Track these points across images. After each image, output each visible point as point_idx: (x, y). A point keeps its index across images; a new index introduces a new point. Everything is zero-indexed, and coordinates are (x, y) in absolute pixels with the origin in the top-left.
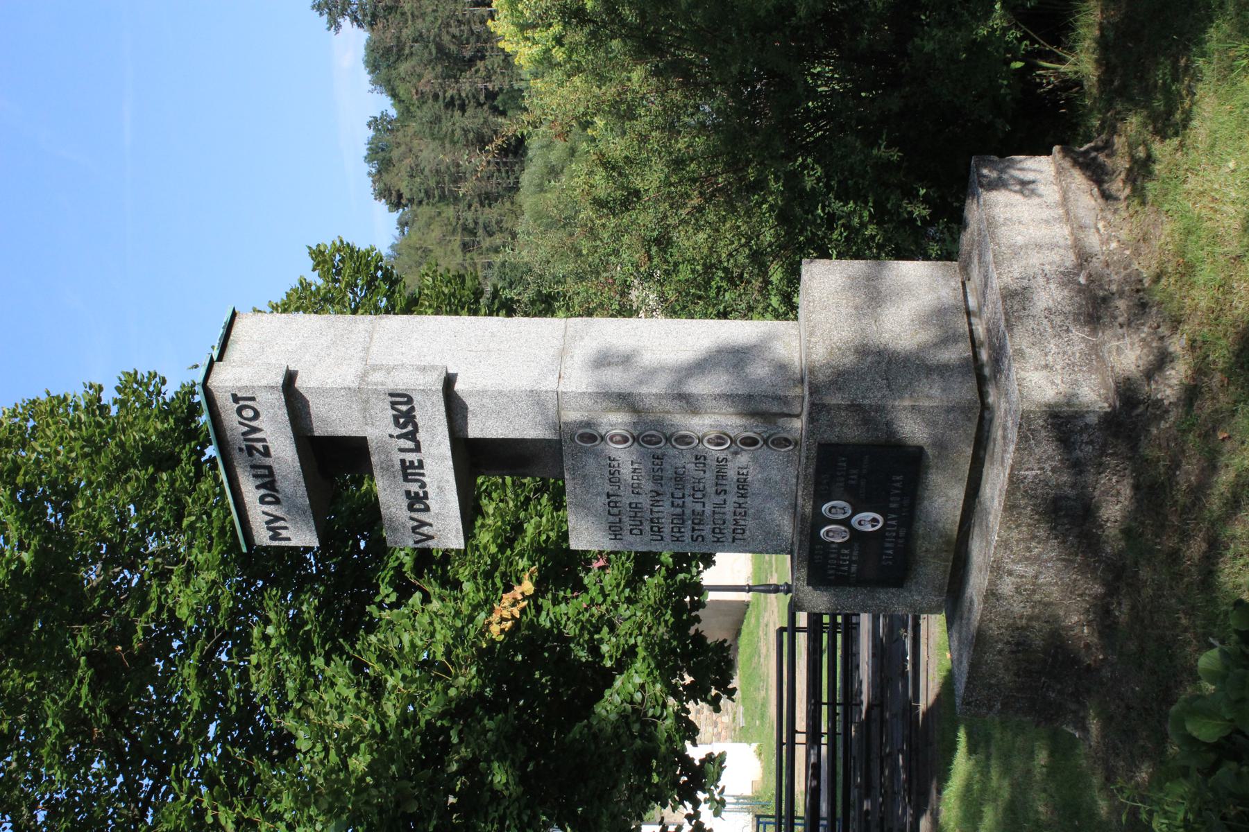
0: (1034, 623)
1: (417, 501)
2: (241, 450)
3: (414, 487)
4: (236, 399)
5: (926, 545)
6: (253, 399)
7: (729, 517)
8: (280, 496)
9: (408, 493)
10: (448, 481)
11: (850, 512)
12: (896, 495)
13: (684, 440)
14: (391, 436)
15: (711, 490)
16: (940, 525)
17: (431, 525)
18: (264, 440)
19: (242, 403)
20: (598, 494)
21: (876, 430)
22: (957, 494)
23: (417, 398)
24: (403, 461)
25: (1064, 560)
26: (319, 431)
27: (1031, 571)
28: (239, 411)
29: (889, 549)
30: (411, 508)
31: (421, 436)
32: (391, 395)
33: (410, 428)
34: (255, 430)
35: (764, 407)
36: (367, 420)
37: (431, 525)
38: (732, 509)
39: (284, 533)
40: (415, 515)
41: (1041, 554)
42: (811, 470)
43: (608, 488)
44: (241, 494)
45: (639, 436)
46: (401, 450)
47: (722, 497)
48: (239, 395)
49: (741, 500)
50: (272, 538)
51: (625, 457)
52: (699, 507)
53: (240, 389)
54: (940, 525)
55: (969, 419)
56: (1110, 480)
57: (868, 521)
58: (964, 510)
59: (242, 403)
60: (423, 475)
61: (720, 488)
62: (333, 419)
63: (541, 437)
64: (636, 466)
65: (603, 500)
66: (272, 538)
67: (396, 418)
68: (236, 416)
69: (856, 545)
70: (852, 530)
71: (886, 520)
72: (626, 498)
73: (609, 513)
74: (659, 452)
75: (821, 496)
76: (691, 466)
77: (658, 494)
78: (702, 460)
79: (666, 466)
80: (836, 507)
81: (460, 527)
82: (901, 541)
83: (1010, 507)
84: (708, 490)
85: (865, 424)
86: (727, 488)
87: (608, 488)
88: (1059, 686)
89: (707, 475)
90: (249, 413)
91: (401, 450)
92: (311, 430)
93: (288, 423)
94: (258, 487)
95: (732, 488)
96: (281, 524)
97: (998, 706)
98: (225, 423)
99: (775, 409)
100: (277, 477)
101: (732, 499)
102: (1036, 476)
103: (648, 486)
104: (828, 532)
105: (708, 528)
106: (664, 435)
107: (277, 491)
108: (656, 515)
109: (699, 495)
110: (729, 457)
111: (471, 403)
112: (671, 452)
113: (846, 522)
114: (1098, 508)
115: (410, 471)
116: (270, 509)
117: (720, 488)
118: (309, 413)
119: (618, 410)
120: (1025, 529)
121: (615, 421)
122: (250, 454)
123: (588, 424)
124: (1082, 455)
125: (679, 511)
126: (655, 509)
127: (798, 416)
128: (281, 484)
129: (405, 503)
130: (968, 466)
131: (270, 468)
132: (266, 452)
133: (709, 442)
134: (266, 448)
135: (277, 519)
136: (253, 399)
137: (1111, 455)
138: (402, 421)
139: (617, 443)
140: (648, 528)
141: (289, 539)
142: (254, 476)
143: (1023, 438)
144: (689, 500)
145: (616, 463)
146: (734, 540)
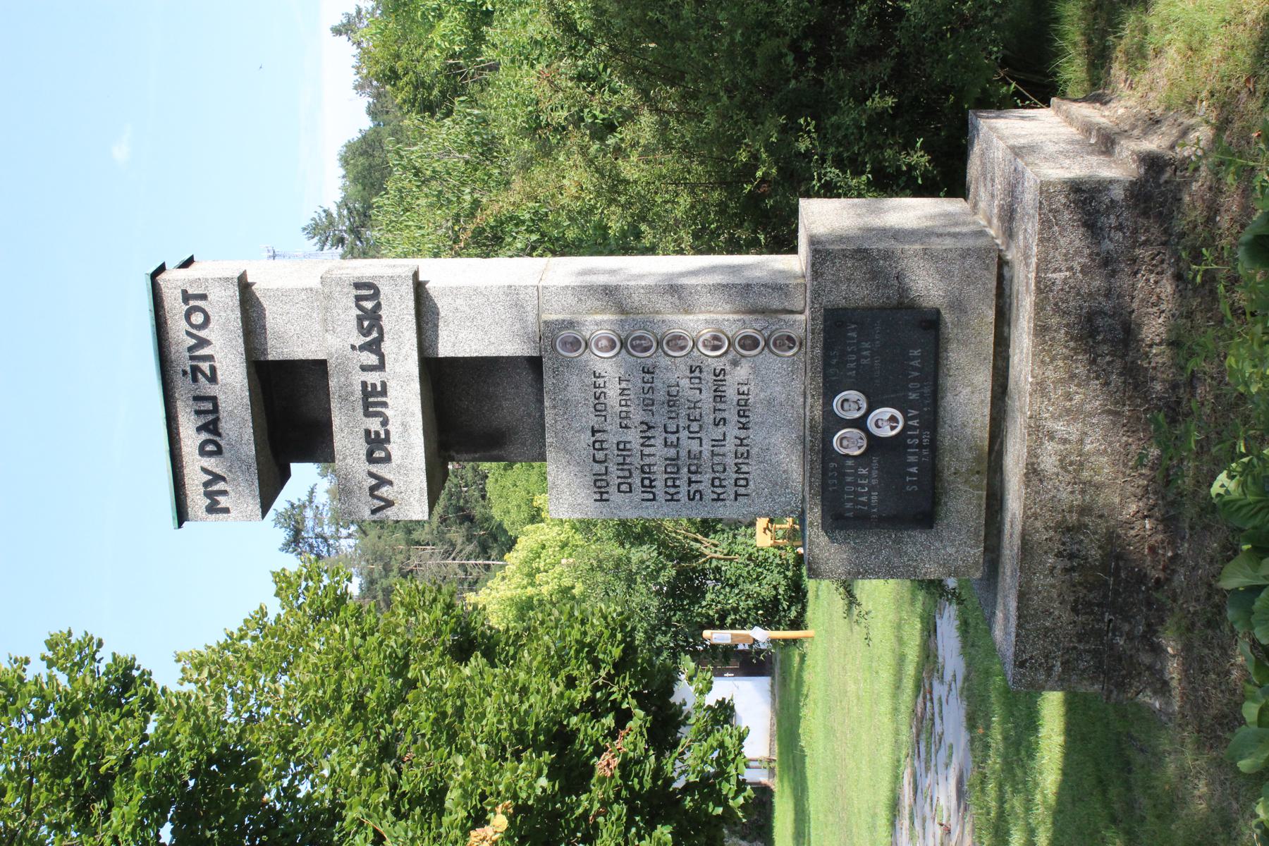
0: (1086, 519)
2: (185, 373)
3: (374, 425)
4: (186, 297)
5: (954, 465)
6: (203, 297)
7: (730, 461)
8: (222, 443)
9: (368, 432)
10: (413, 414)
11: (864, 406)
12: (914, 380)
13: (676, 342)
14: (353, 347)
15: (709, 419)
16: (968, 431)
17: (391, 483)
18: (210, 358)
19: (192, 303)
20: (582, 430)
21: (886, 286)
22: (983, 379)
23: (384, 290)
24: (364, 384)
25: (1109, 412)
26: (273, 355)
27: (1074, 431)
28: (188, 316)
29: (911, 465)
30: (371, 459)
31: (386, 346)
32: (358, 286)
33: (375, 335)
34: (203, 343)
35: (763, 302)
36: (327, 325)
37: (391, 483)
38: (733, 448)
39: (223, 501)
40: (375, 469)
41: (1083, 402)
42: (818, 351)
43: (593, 421)
44: (179, 441)
45: (627, 338)
46: (364, 368)
47: (721, 429)
48: (190, 292)
49: (743, 434)
51: (607, 367)
55: (987, 269)
56: (1148, 280)
57: (886, 422)
58: (993, 419)
59: (192, 303)
60: (385, 404)
61: (719, 415)
62: (292, 339)
63: (519, 354)
64: (624, 385)
65: (587, 438)
67: (360, 319)
68: (184, 325)
69: (875, 460)
71: (906, 419)
73: (595, 460)
74: (649, 362)
76: (685, 383)
77: (650, 428)
78: (697, 374)
79: (658, 384)
80: (850, 402)
81: (425, 485)
82: (925, 452)
83: (1041, 330)
84: (705, 418)
85: (873, 279)
86: (725, 415)
87: (593, 421)
88: (1126, 627)
89: (703, 396)
90: (198, 318)
91: (364, 368)
92: (265, 352)
93: (240, 332)
94: (199, 429)
95: (732, 416)
96: (220, 486)
97: (1058, 668)
99: (776, 304)
100: (223, 414)
101: (732, 431)
102: (1065, 281)
103: (637, 415)
104: (842, 439)
105: (707, 477)
106: (655, 335)
107: (219, 435)
108: (647, 461)
109: (695, 426)
110: (728, 368)
111: (443, 304)
112: (664, 361)
113: (860, 423)
114: (1139, 326)
115: (372, 399)
116: (210, 463)
118: (264, 327)
119: (603, 311)
120: (1060, 363)
121: (598, 324)
122: (195, 380)
123: (571, 324)
124: (1112, 247)
126: (647, 451)
127: (801, 313)
128: (224, 426)
129: (362, 448)
130: (992, 338)
131: (214, 399)
132: (213, 379)
133: (705, 346)
134: (213, 369)
135: (218, 478)
136: (203, 297)
137: (1145, 243)
138: (366, 324)
139: (601, 350)
140: (638, 481)
142: (198, 413)
143: (1045, 224)
144: (684, 434)
145: (600, 381)
146: (737, 495)
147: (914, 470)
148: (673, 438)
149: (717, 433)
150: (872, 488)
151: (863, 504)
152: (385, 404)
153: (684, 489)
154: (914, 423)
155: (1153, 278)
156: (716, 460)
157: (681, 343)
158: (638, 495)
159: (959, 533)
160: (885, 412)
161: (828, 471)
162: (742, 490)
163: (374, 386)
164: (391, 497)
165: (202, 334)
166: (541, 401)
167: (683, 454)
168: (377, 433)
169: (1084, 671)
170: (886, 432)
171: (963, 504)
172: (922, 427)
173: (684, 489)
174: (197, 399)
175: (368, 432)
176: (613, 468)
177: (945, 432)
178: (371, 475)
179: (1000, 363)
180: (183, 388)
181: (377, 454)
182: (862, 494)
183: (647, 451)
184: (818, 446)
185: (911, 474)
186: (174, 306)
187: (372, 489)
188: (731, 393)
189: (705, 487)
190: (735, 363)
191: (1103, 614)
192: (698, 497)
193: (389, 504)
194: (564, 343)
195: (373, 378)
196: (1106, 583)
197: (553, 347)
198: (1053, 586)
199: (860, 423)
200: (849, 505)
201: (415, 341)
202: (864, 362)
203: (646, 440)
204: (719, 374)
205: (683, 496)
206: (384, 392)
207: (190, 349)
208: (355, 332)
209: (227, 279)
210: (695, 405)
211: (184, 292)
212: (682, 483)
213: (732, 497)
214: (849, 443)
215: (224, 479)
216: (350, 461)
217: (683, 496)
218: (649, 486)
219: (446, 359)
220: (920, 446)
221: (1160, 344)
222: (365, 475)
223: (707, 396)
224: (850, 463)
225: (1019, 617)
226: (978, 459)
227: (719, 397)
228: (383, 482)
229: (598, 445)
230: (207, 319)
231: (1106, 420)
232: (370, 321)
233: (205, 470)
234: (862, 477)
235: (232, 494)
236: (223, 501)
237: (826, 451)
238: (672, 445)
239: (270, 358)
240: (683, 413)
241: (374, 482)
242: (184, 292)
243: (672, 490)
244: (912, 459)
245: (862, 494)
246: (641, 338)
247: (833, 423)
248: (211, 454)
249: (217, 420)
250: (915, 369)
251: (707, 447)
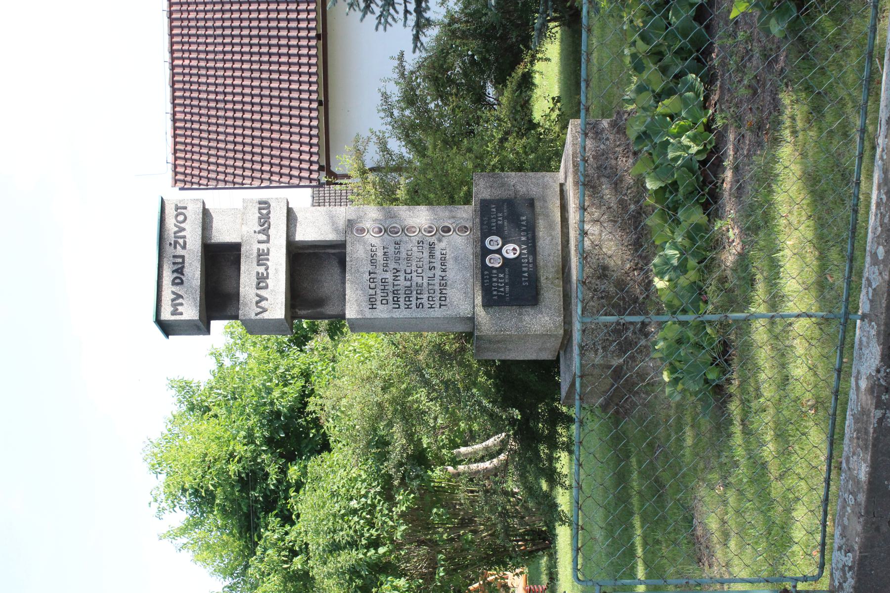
1: (261, 281)
2: (170, 244)
3: (261, 269)
6: (185, 208)
7: (437, 287)
8: (184, 279)
9: (258, 273)
13: (410, 229)
14: (255, 232)
15: (426, 267)
18: (184, 237)
23: (273, 204)
25: (612, 221)
29: (525, 272)
31: (271, 232)
32: (260, 203)
33: (266, 225)
39: (180, 309)
40: (260, 292)
46: (259, 242)
47: (433, 272)
49: (443, 274)
50: (173, 314)
52: (419, 280)
53: (180, 201)
57: (511, 251)
60: (268, 260)
61: (432, 265)
62: (223, 234)
65: (366, 276)
66: (173, 314)
67: (260, 218)
70: (504, 258)
71: (521, 250)
72: (380, 275)
74: (398, 239)
75: (484, 236)
76: (415, 249)
79: (402, 249)
80: (493, 242)
82: (531, 266)
90: (181, 218)
92: (210, 239)
94: (173, 272)
95: (437, 265)
96: (180, 301)
97: (601, 351)
98: (167, 225)
100: (186, 264)
101: (438, 273)
105: (425, 296)
108: (396, 288)
109: (420, 271)
112: (405, 239)
113: (499, 251)
115: (262, 257)
116: (176, 289)
117: (432, 265)
122: (175, 247)
125: (408, 283)
126: (396, 283)
129: (254, 281)
131: (183, 257)
132: (184, 247)
134: (185, 243)
135: (179, 296)
136: (185, 208)
137: (619, 145)
141: (181, 314)
142: (174, 263)
145: (374, 248)
146: (440, 305)
147: (526, 275)
148: (409, 276)
149: (431, 274)
150: (506, 284)
151: (502, 292)
152: (268, 260)
153: (414, 302)
154: (525, 251)
155: (624, 159)
156: (430, 287)
157: (413, 230)
158: (391, 305)
159: (550, 309)
160: (510, 246)
161: (486, 277)
162: (443, 303)
163: (263, 250)
164: (266, 307)
165: (182, 225)
166: (344, 283)
167: (414, 284)
168: (263, 274)
170: (511, 256)
171: (551, 294)
172: (528, 253)
173: (414, 302)
174: (174, 257)
175: (258, 273)
176: (379, 292)
177: (540, 258)
178: (257, 295)
179: (565, 230)
180: (169, 251)
181: (261, 285)
182: (501, 287)
183: (396, 283)
184: (479, 266)
185: (525, 277)
186: (170, 212)
187: (257, 303)
188: (438, 254)
189: (425, 301)
190: (440, 240)
193: (265, 310)
194: (357, 230)
195: (263, 246)
196: (619, 305)
197: (352, 232)
198: (594, 307)
199: (499, 251)
200: (495, 293)
201: (285, 229)
202: (500, 222)
203: (396, 277)
204: (432, 246)
205: (413, 306)
206: (268, 254)
207: (175, 233)
208: (257, 224)
209: (197, 200)
210: (420, 260)
211: (176, 205)
212: (413, 299)
214: (494, 262)
215: (182, 297)
216: (247, 288)
217: (413, 306)
218: (396, 301)
220: (528, 263)
222: (254, 295)
223: (426, 254)
224: (495, 271)
226: (557, 272)
227: (432, 256)
228: (262, 299)
229: (372, 280)
230: (185, 218)
231: (611, 224)
232: (265, 221)
233: (173, 293)
234: (501, 278)
235: (185, 305)
236: (180, 309)
237: (484, 266)
239: (213, 241)
240: (414, 264)
241: (258, 299)
242: (176, 205)
243: (408, 303)
244: (525, 269)
245: (501, 287)
246: (394, 227)
247: (485, 252)
248: (177, 284)
249: (183, 267)
250: (524, 226)
251: (425, 281)
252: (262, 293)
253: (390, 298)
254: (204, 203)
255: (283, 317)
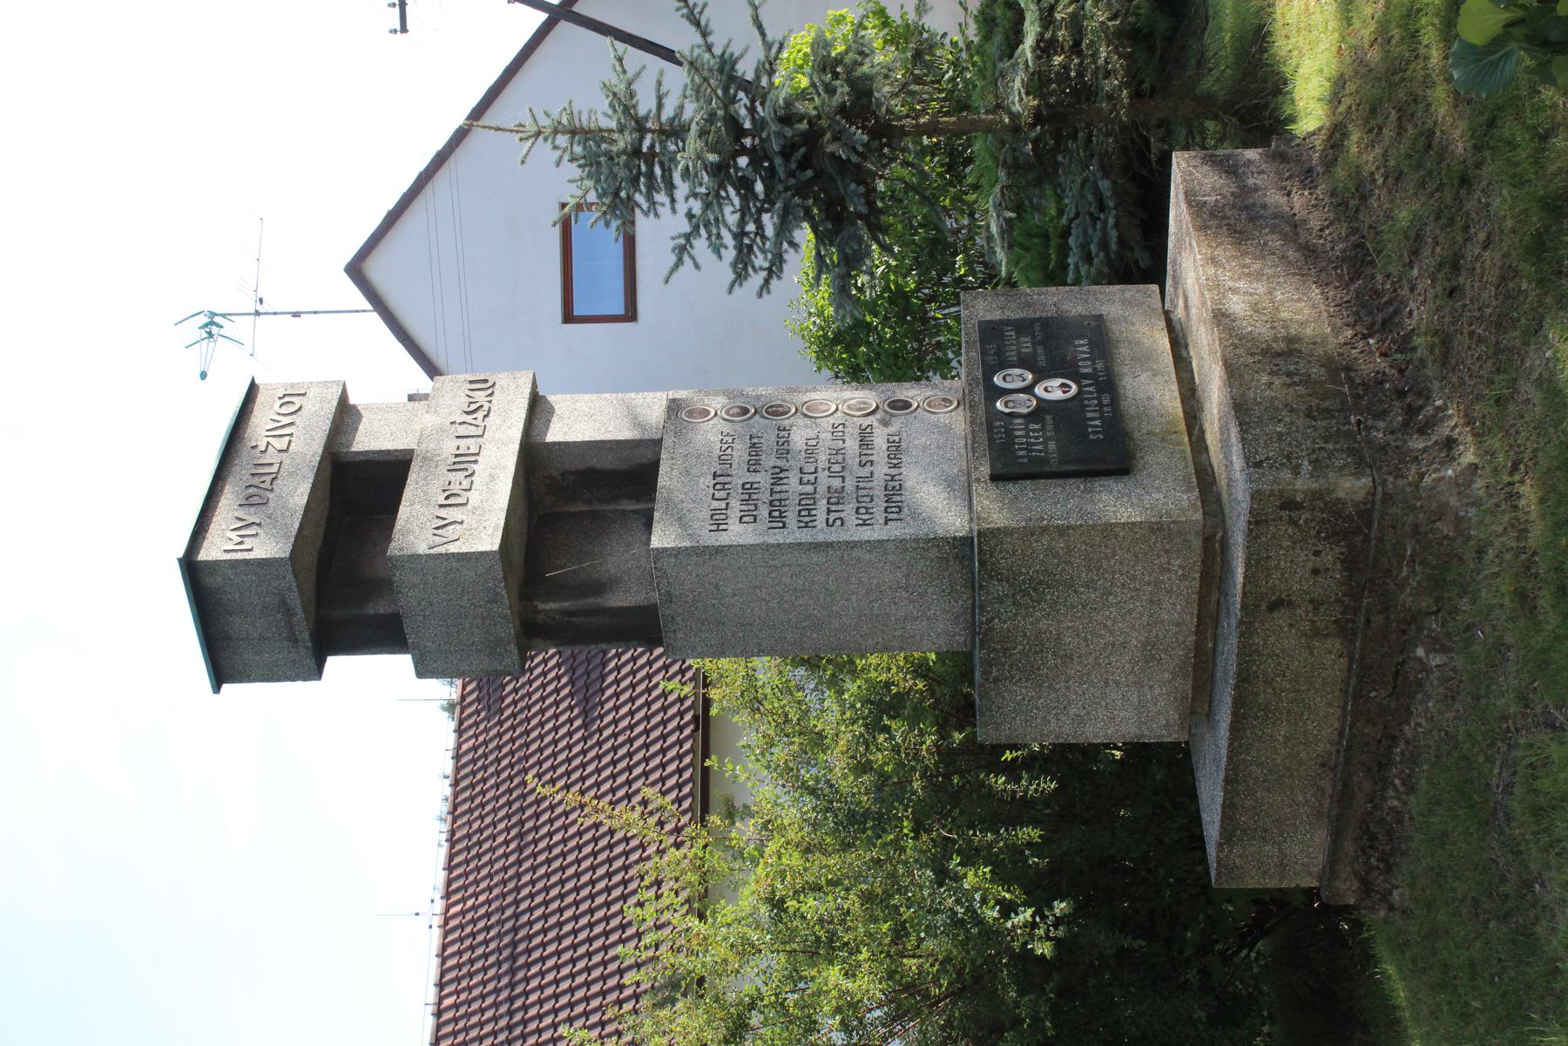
47: (868, 469)
49: (894, 472)
54: (1156, 403)
61: (864, 459)
108: (778, 496)
109: (836, 468)
125: (809, 489)
126: (777, 488)
169: (1342, 468)
191: (1347, 418)
192: (838, 522)
213: (882, 521)
219: (554, 443)
221: (1331, 224)
224: (1019, 421)
225: (1241, 424)
238: (808, 482)
252: (452, 514)
253: (764, 512)
254: (344, 391)
255: (496, 547)
